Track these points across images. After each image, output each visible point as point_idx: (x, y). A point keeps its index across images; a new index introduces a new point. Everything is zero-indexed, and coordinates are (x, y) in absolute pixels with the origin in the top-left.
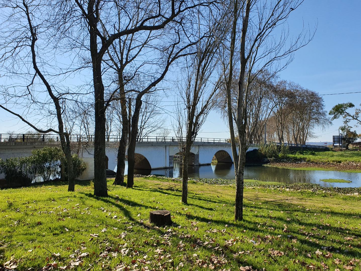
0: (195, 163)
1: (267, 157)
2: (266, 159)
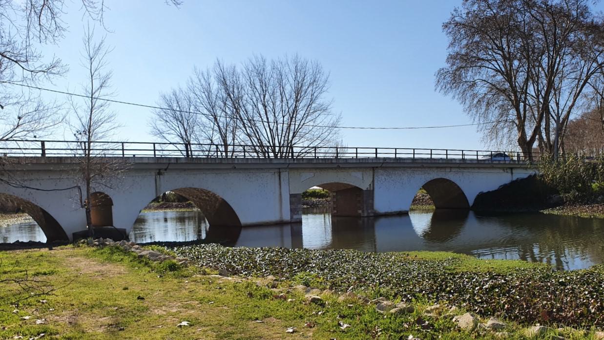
0: (363, 211)
1: (558, 192)
2: (555, 197)
